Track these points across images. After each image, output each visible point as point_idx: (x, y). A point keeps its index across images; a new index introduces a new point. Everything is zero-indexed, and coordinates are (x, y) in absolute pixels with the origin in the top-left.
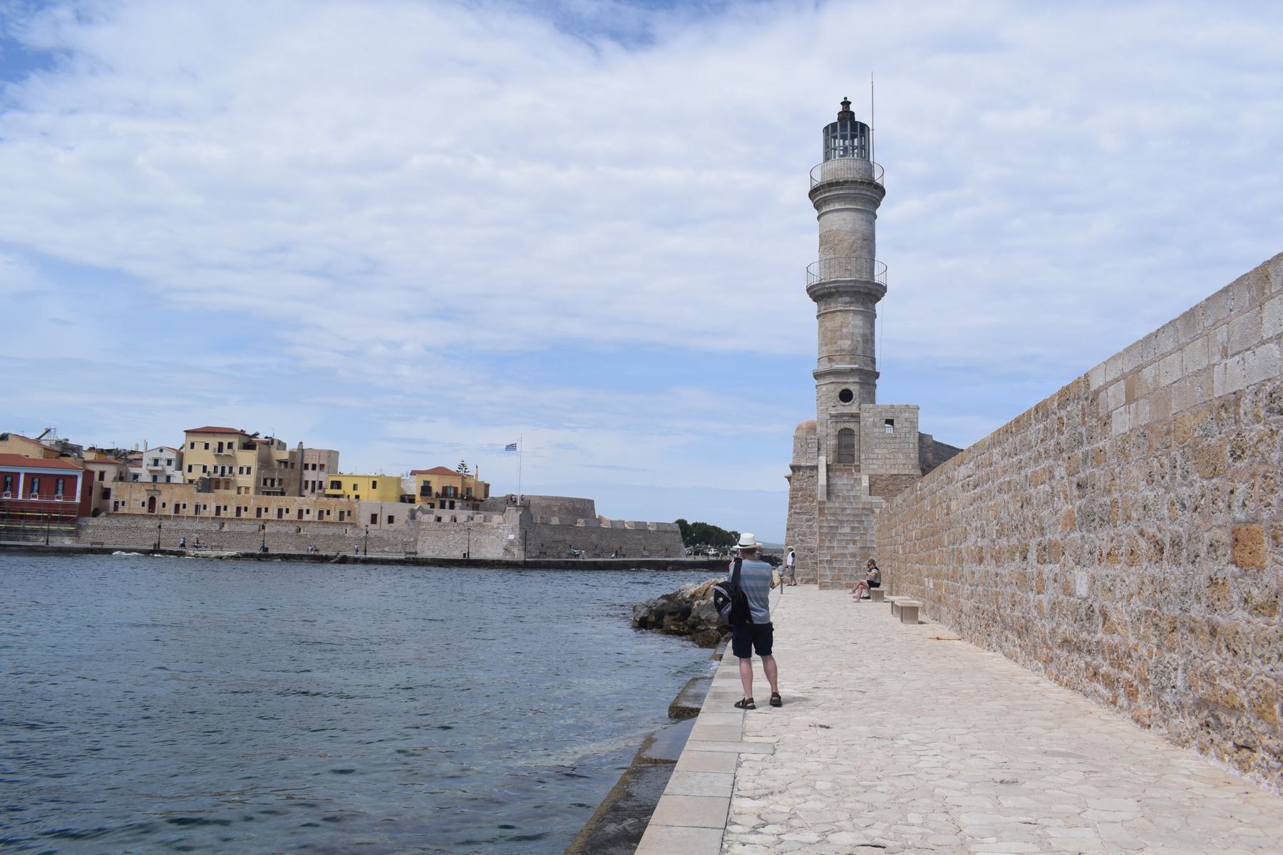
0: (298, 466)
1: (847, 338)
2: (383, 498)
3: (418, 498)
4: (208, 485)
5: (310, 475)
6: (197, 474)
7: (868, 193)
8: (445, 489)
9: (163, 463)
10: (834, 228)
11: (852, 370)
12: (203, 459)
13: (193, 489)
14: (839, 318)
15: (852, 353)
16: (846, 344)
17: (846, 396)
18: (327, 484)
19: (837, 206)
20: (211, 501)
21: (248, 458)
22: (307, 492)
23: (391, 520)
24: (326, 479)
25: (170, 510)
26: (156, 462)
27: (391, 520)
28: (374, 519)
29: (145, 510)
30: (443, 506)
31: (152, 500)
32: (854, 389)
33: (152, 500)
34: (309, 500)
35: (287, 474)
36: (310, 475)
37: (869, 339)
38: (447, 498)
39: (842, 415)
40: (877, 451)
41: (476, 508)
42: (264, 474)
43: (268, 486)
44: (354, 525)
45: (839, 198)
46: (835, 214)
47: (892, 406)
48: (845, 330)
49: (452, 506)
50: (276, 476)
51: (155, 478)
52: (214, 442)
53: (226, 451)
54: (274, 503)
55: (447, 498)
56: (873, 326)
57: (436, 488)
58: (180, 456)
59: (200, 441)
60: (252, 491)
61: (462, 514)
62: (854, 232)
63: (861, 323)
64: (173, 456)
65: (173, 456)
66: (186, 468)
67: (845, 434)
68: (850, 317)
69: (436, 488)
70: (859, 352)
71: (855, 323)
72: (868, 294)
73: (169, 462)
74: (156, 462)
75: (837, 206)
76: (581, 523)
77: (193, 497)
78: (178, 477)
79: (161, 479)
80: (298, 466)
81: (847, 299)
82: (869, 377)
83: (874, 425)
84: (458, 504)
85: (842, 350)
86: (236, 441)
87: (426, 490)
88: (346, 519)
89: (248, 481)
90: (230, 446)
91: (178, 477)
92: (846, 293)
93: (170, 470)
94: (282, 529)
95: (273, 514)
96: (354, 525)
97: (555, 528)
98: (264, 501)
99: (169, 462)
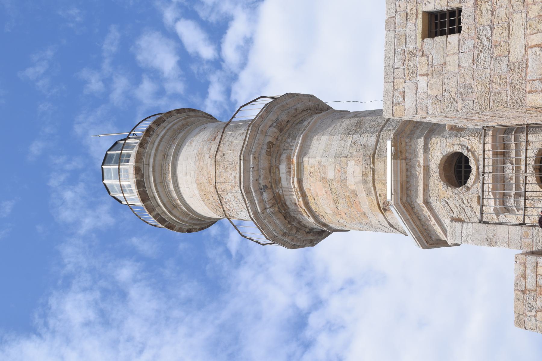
1: (342, 170)
10: (197, 192)
11: (395, 156)
14: (312, 185)
15: (373, 156)
16: (355, 170)
17: (457, 170)
19: (171, 186)
32: (441, 148)
37: (360, 120)
39: (501, 181)
40: (517, 53)
45: (162, 183)
46: (182, 189)
47: (391, 24)
48: (331, 174)
56: (343, 114)
62: (200, 154)
63: (324, 138)
68: (309, 162)
70: (370, 140)
75: (171, 186)
81: (283, 168)
83: (437, 71)
85: (365, 182)
92: (272, 170)
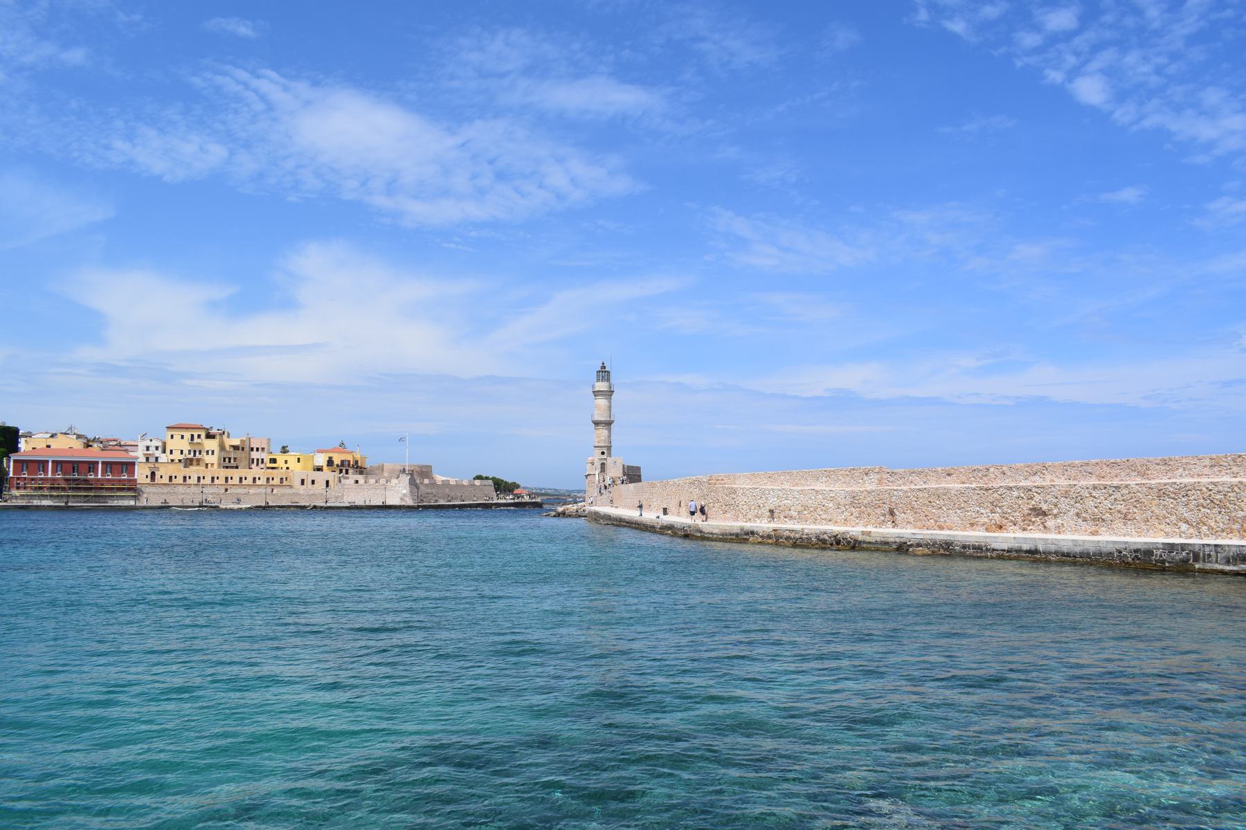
0: (247, 449)
2: (304, 469)
3: (325, 468)
4: (188, 463)
5: (255, 455)
6: (177, 456)
7: (609, 394)
8: (342, 462)
9: (152, 450)
12: (179, 444)
13: (181, 466)
18: (267, 460)
20: (194, 472)
21: (212, 445)
22: (254, 466)
23: (313, 482)
24: (266, 457)
25: (166, 480)
26: (148, 448)
27: (313, 482)
28: (303, 482)
29: (148, 480)
30: (341, 471)
31: (153, 474)
33: (153, 474)
34: (256, 471)
35: (238, 454)
36: (255, 455)
38: (344, 467)
41: (361, 473)
42: (224, 454)
43: (228, 462)
44: (291, 487)
49: (347, 472)
50: (232, 456)
51: (147, 459)
52: (187, 435)
53: (196, 440)
54: (236, 474)
55: (344, 467)
57: (337, 461)
58: (164, 444)
59: (177, 434)
60: (216, 466)
61: (353, 476)
64: (159, 444)
65: (159, 444)
66: (168, 451)
67: (603, 465)
69: (337, 461)
71: (605, 432)
72: (608, 424)
73: (157, 448)
74: (148, 448)
76: (426, 481)
77: (179, 471)
78: (164, 458)
79: (152, 460)
80: (247, 449)
82: (609, 448)
84: (351, 471)
86: (203, 436)
87: (330, 462)
88: (285, 483)
89: (212, 459)
90: (199, 436)
91: (164, 458)
93: (158, 453)
94: (241, 491)
95: (236, 481)
96: (291, 487)
97: (426, 485)
98: (229, 472)
99: (157, 448)
